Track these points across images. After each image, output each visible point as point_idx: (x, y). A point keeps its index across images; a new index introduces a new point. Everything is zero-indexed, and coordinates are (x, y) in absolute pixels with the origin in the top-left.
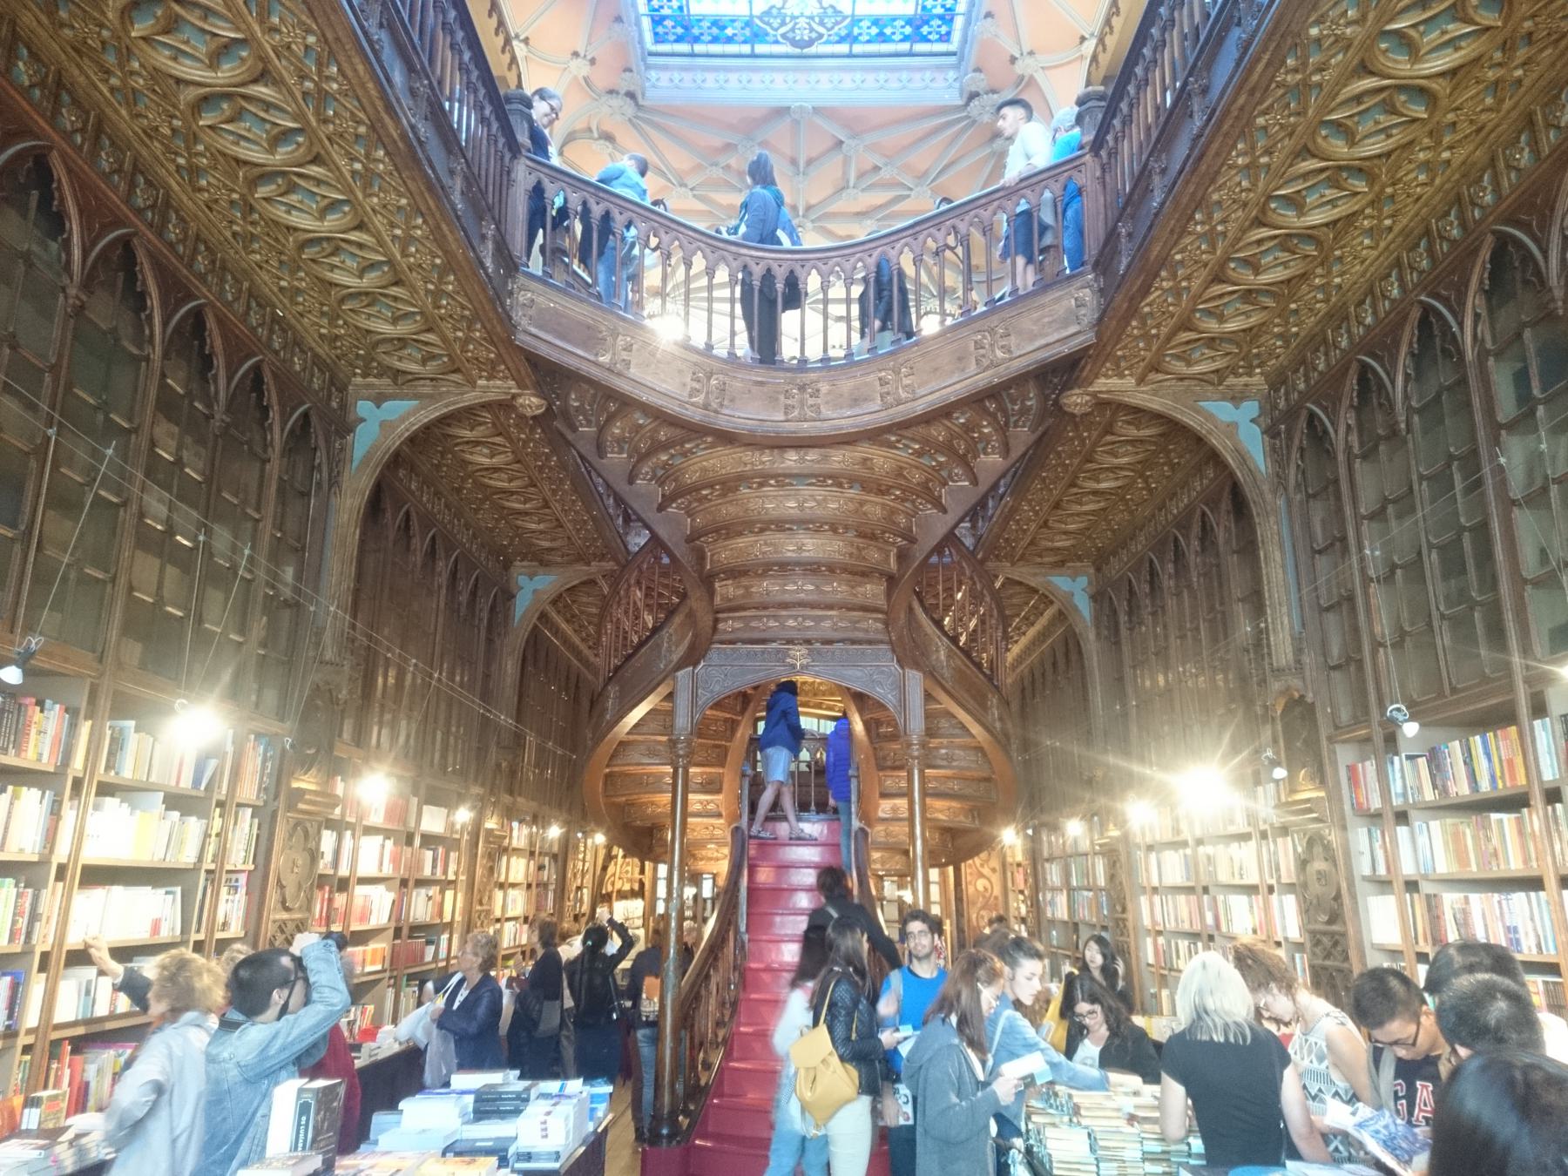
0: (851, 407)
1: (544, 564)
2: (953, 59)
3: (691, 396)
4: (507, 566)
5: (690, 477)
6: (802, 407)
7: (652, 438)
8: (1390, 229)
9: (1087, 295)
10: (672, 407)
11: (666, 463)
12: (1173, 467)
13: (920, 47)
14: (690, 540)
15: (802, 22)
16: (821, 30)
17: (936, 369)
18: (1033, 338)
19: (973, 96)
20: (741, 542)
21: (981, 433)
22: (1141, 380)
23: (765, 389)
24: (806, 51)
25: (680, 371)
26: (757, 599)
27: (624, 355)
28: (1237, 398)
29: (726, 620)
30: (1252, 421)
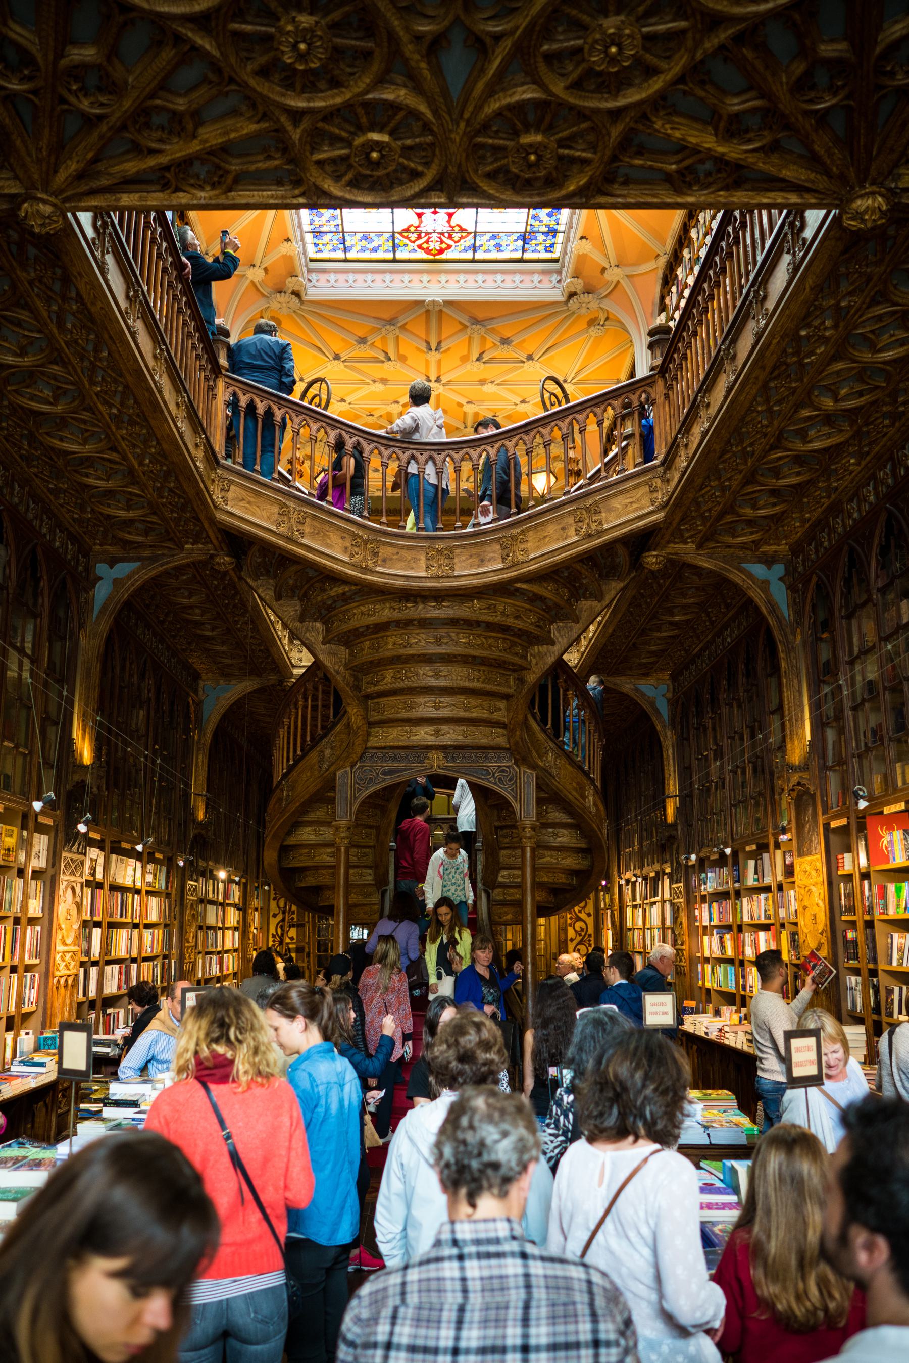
8: (868, 453)
15: (435, 237)
22: (700, 546)
24: (438, 257)
28: (769, 561)
30: (780, 579)
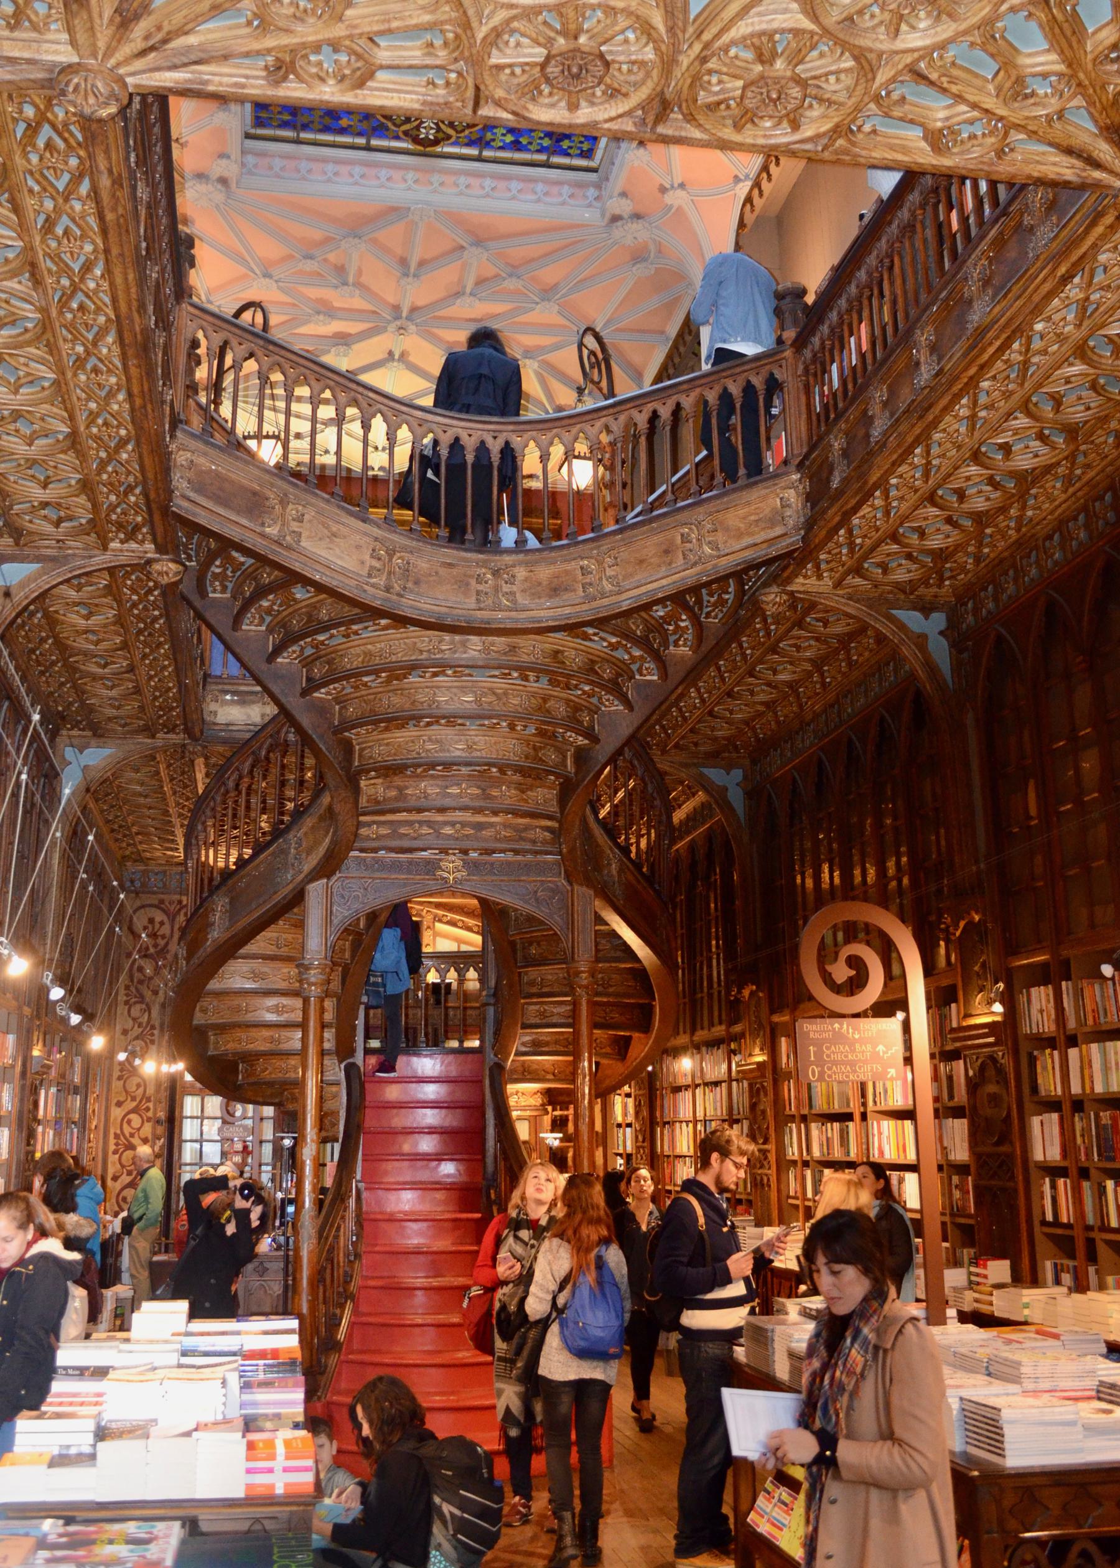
0: (551, 597)
2: (593, 176)
3: (370, 576)
5: (353, 659)
7: (310, 616)
9: (791, 495)
10: (348, 587)
11: (322, 643)
12: (850, 664)
13: (556, 160)
16: (450, 132)
17: (641, 562)
18: (740, 535)
19: (615, 219)
20: (400, 736)
21: (677, 627)
22: (838, 584)
23: (455, 571)
25: (358, 547)
26: (412, 803)
27: (295, 526)
28: (926, 609)
29: (369, 824)
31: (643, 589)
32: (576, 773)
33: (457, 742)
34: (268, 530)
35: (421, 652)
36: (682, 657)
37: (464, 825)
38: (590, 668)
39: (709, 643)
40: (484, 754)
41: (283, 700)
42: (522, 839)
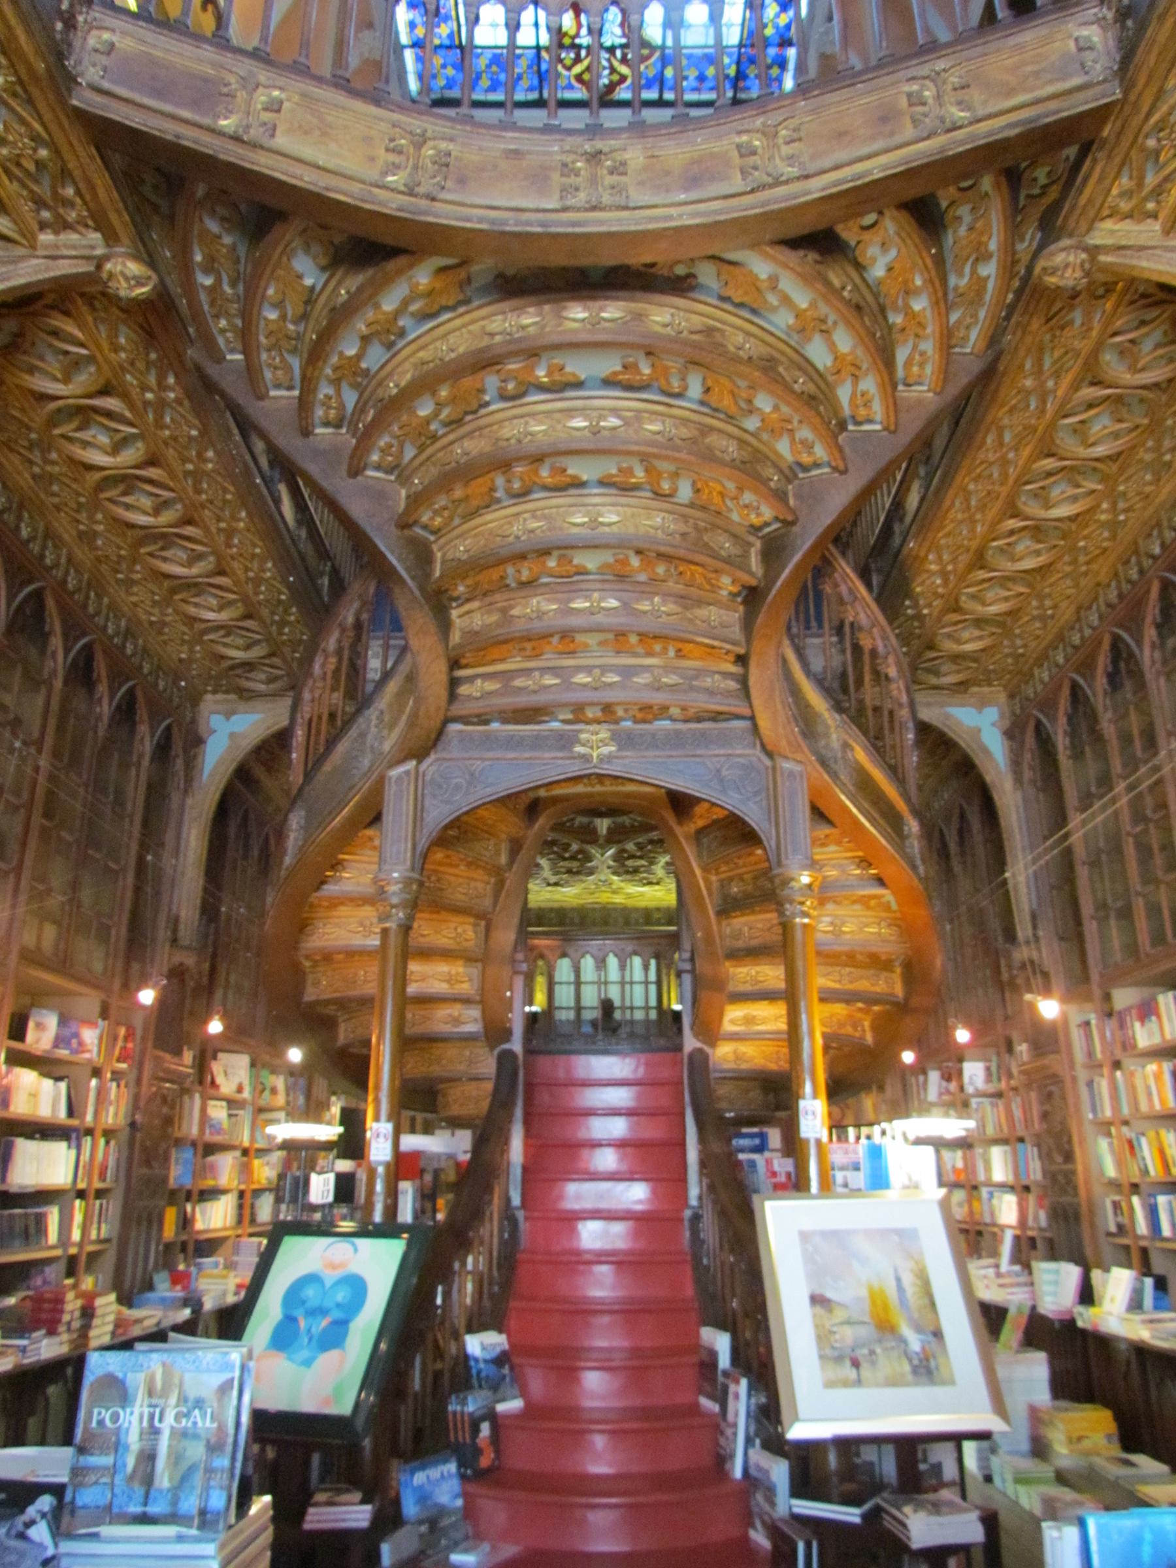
0: (686, 189)
1: (246, 695)
4: (195, 700)
6: (594, 181)
14: (405, 523)
18: (1011, 92)
25: (367, 140)
26: (519, 626)
27: (266, 116)
29: (471, 679)
31: (846, 172)
32: (766, 575)
33: (573, 514)
34: (223, 123)
35: (492, 335)
36: (920, 402)
37: (604, 669)
38: (768, 367)
39: (963, 380)
40: (615, 529)
41: (324, 484)
42: (692, 688)
